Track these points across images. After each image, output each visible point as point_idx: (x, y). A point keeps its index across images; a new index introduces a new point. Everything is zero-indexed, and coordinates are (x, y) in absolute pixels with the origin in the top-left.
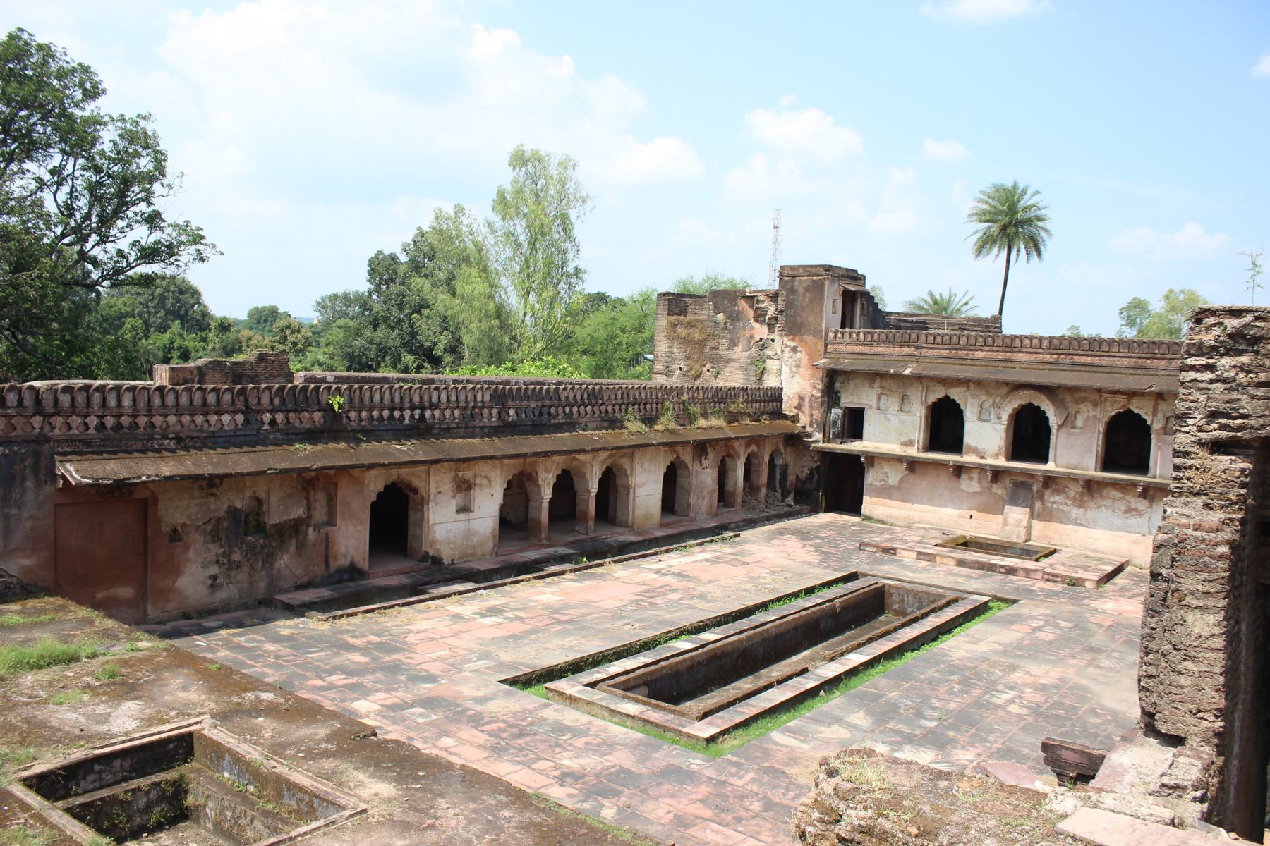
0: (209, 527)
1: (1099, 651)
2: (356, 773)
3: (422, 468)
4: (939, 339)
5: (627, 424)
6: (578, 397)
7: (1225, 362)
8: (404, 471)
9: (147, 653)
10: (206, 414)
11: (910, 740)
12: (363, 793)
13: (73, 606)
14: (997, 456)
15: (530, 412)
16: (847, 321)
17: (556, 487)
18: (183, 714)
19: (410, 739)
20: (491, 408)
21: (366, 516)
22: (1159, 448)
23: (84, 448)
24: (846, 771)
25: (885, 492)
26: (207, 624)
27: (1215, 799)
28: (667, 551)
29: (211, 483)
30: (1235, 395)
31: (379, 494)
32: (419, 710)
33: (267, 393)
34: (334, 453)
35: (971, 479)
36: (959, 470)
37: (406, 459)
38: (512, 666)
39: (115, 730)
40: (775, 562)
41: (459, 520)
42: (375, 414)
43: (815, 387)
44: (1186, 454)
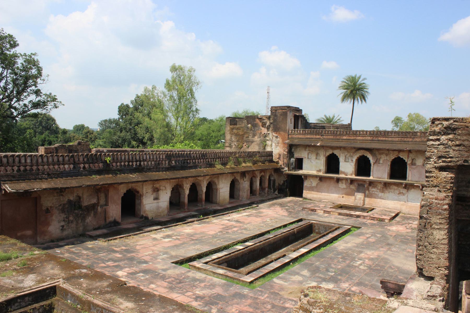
0: (61, 207)
1: (391, 245)
2: (119, 299)
3: (140, 184)
4: (329, 132)
5: (216, 166)
6: (198, 156)
7: (443, 137)
8: (133, 185)
9: (38, 256)
10: (59, 165)
11: (324, 280)
12: (121, 306)
13: (9, 239)
14: (352, 175)
16: (296, 126)
17: (190, 190)
18: (52, 279)
19: (139, 285)
20: (165, 161)
21: (120, 202)
22: (410, 170)
23: (12, 178)
24: (311, 295)
25: (311, 189)
26: (60, 244)
27: (446, 300)
28: (232, 212)
29: (61, 191)
30: (448, 150)
31: (125, 194)
32: (142, 274)
33: (82, 156)
34: (107, 179)
35: (342, 183)
36: (338, 180)
37: (134, 180)
38: (176, 257)
39: (26, 285)
40: (271, 216)
41: (154, 203)
42: (123, 164)
43: (285, 151)
44: (430, 172)
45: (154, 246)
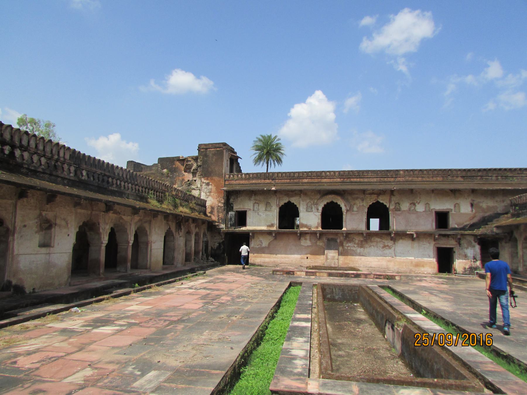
5: (150, 200)
6: (125, 176)
15: (96, 176)
16: (231, 171)
20: (69, 165)
22: (394, 217)
28: (180, 280)
35: (306, 239)
43: (220, 202)
45: (81, 349)
